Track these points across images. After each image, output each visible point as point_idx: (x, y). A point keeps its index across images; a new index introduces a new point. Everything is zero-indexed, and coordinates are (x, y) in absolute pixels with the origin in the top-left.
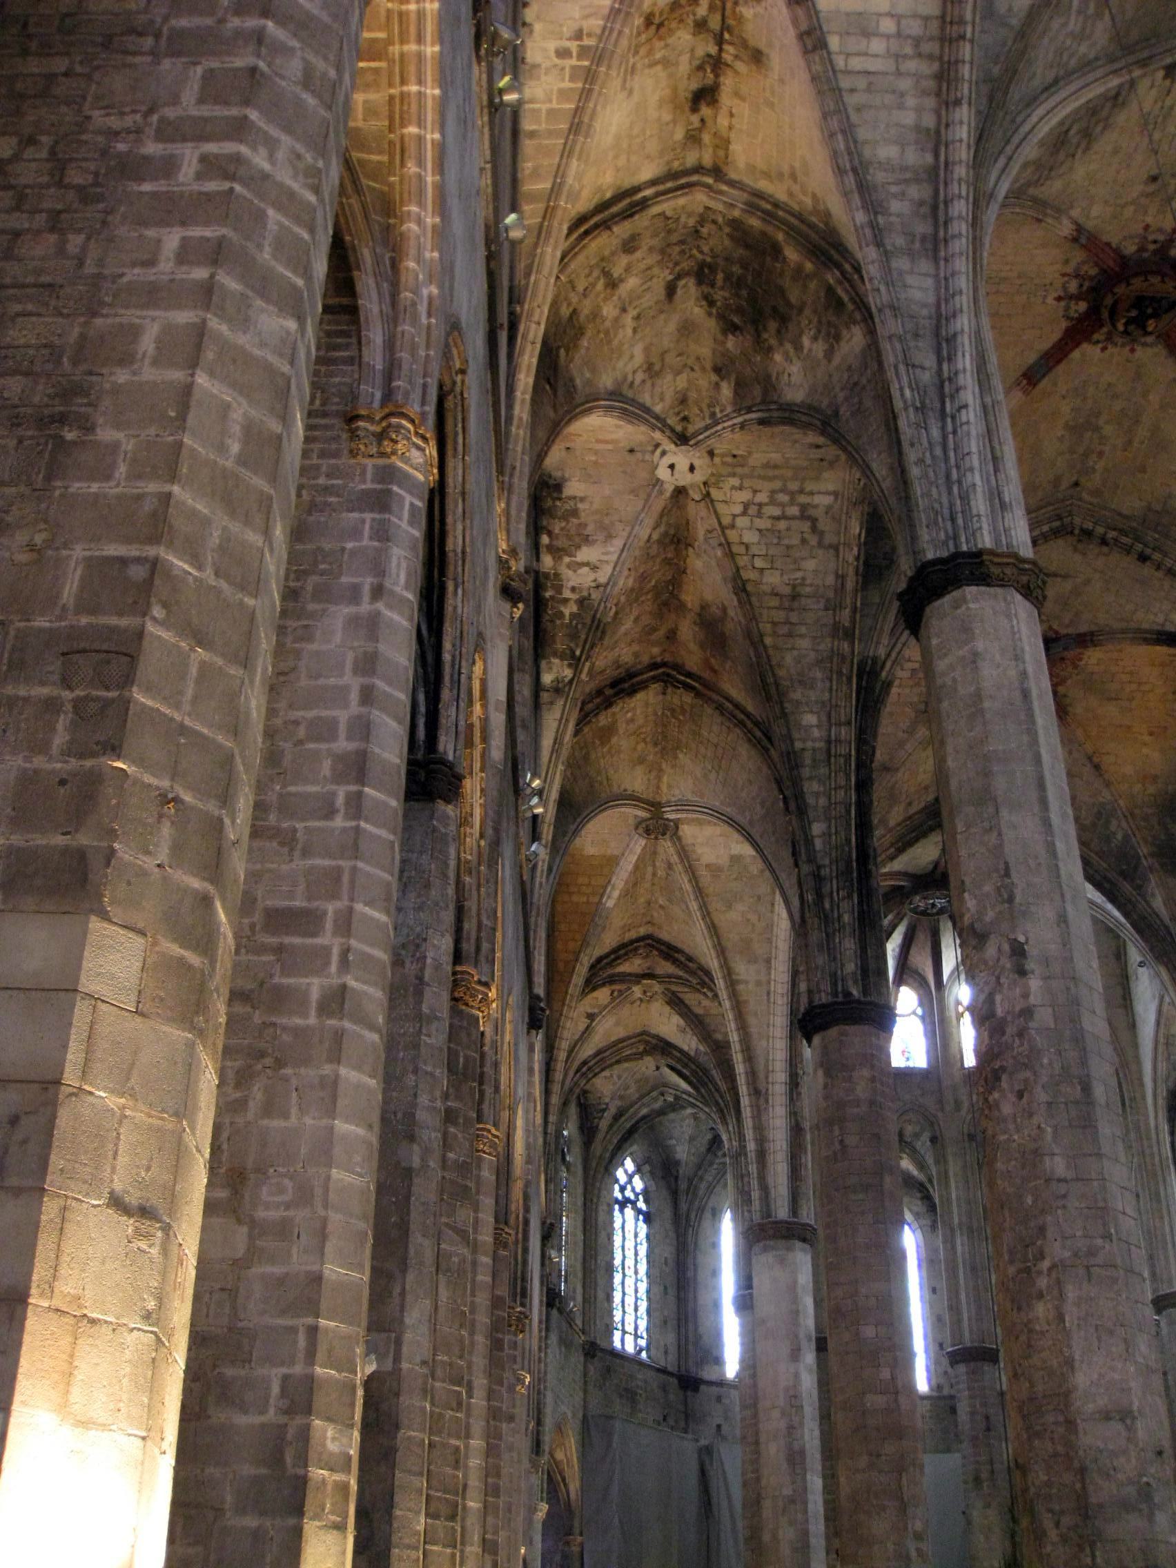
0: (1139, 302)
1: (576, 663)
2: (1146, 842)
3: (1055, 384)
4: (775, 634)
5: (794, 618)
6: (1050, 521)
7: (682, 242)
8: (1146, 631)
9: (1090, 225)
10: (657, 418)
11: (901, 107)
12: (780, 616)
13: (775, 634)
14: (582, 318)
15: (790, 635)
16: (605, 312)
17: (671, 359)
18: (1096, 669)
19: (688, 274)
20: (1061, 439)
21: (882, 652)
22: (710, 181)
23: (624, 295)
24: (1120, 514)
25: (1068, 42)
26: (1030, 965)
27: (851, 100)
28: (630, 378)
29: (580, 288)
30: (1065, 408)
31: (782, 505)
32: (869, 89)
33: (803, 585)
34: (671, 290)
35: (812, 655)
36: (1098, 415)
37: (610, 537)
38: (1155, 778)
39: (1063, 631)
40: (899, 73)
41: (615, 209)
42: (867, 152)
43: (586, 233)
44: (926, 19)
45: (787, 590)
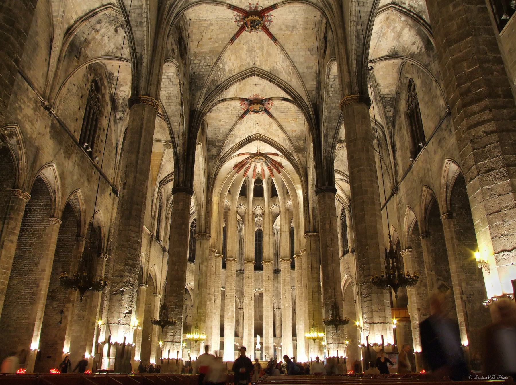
0: (252, 22)
1: (123, 113)
2: (293, 146)
5: (170, 101)
6: (249, 73)
7: (113, 20)
8: (280, 97)
9: (234, 4)
10: (124, 59)
12: (167, 101)
14: (89, 40)
15: (169, 105)
16: (97, 37)
18: (277, 106)
19: (119, 27)
20: (246, 54)
21: (199, 106)
22: (112, 6)
23: (102, 33)
24: (265, 71)
26: (126, 187)
28: (111, 51)
29: (87, 33)
30: (245, 47)
34: (116, 31)
35: (175, 110)
36: (254, 47)
37: (126, 85)
39: (265, 97)
41: (89, 15)
43: (82, 21)
45: (167, 95)
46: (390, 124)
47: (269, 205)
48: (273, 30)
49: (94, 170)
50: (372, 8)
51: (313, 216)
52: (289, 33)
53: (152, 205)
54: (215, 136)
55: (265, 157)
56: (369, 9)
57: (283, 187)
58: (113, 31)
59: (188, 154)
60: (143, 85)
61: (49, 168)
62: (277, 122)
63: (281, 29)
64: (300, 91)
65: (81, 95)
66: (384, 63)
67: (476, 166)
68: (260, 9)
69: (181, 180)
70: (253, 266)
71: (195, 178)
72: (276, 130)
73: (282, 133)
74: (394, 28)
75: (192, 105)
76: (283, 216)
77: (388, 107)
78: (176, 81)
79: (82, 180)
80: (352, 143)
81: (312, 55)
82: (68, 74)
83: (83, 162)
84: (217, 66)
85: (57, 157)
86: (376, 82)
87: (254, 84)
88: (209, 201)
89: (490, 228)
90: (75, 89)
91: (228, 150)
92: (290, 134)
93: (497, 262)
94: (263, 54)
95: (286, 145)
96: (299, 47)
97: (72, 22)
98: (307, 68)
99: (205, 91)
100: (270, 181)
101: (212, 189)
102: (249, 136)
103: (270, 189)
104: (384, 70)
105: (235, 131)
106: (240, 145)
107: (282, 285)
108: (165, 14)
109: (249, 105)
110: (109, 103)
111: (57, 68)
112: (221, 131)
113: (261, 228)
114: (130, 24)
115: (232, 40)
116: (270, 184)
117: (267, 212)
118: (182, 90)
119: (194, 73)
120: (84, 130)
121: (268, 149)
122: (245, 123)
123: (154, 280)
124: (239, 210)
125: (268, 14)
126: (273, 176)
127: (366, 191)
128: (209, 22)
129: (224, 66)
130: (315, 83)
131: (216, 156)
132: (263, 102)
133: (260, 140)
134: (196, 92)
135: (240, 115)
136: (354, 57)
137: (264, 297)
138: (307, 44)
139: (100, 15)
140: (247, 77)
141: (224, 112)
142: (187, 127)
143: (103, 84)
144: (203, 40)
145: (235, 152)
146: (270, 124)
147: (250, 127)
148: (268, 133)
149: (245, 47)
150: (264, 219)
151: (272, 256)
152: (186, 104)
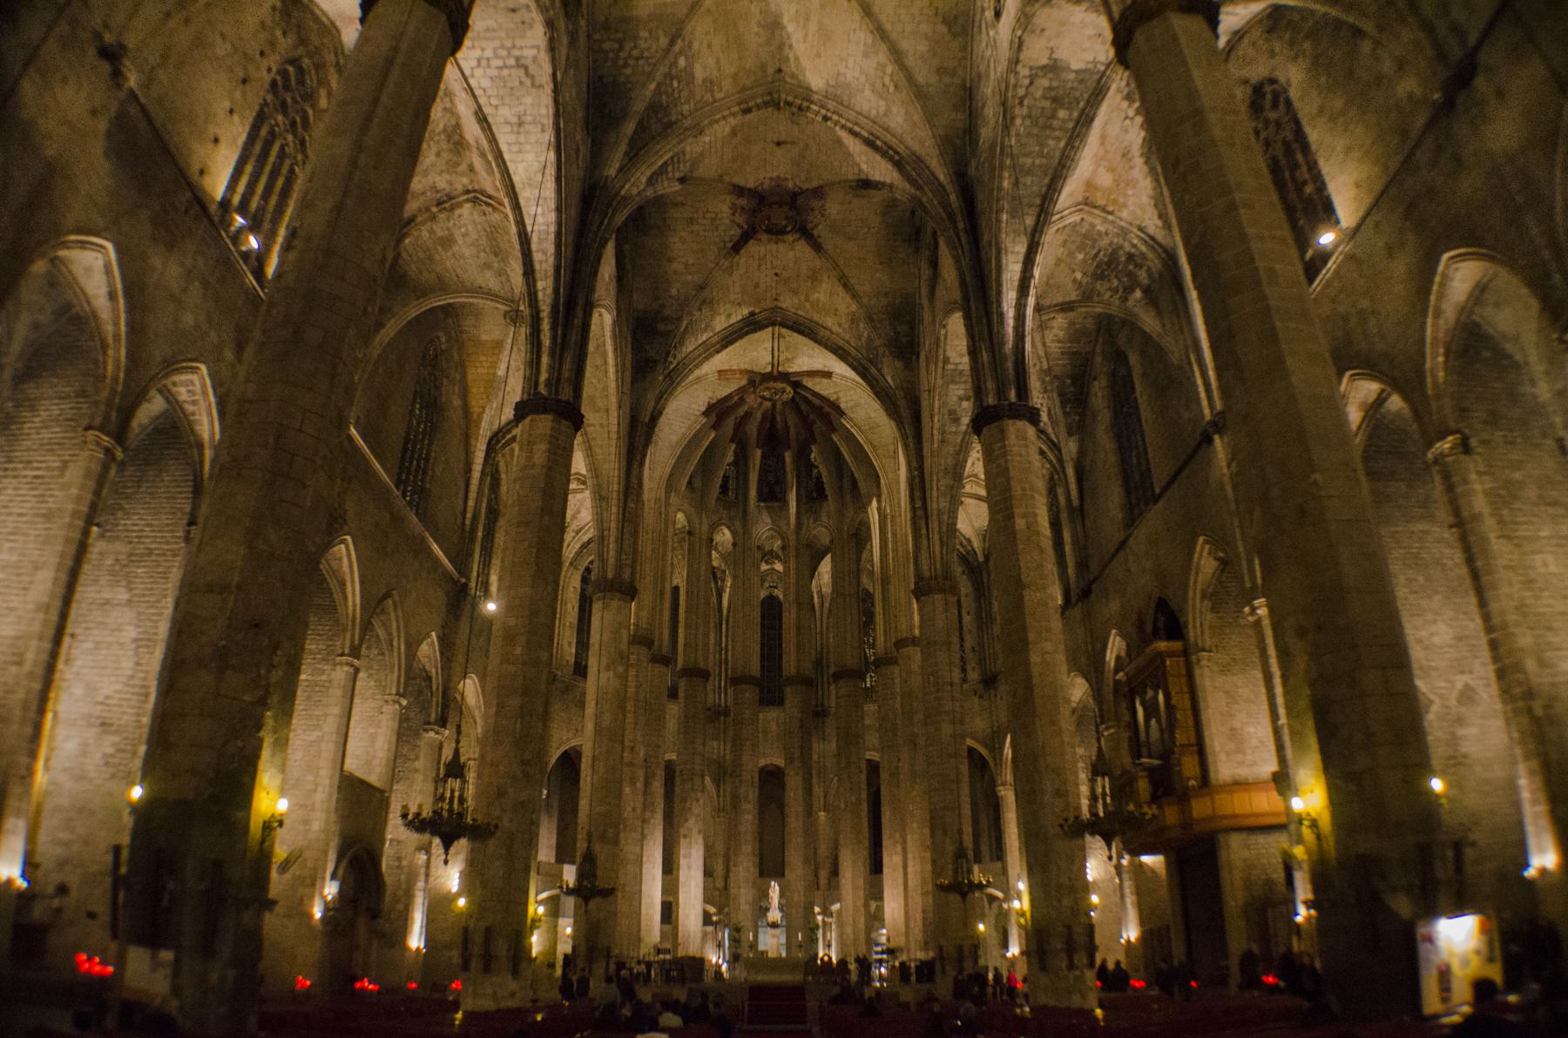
4: (510, 151)
5: (522, 139)
13: (510, 151)
15: (520, 151)
20: (757, 34)
31: (502, 58)
33: (525, 115)
38: (886, 294)
39: (805, 187)
53: (466, 498)
59: (570, 304)
62: (836, 266)
65: (241, 74)
69: (544, 376)
73: (848, 299)
81: (955, 36)
84: (671, 57)
87: (776, 140)
91: (690, 349)
94: (806, 36)
99: (629, 127)
102: (752, 314)
106: (723, 339)
112: (674, 292)
113: (779, 593)
119: (601, 78)
129: (691, 59)
131: (655, 362)
132: (800, 201)
133: (783, 325)
135: (729, 245)
140: (758, 107)
141: (683, 234)
148: (807, 305)
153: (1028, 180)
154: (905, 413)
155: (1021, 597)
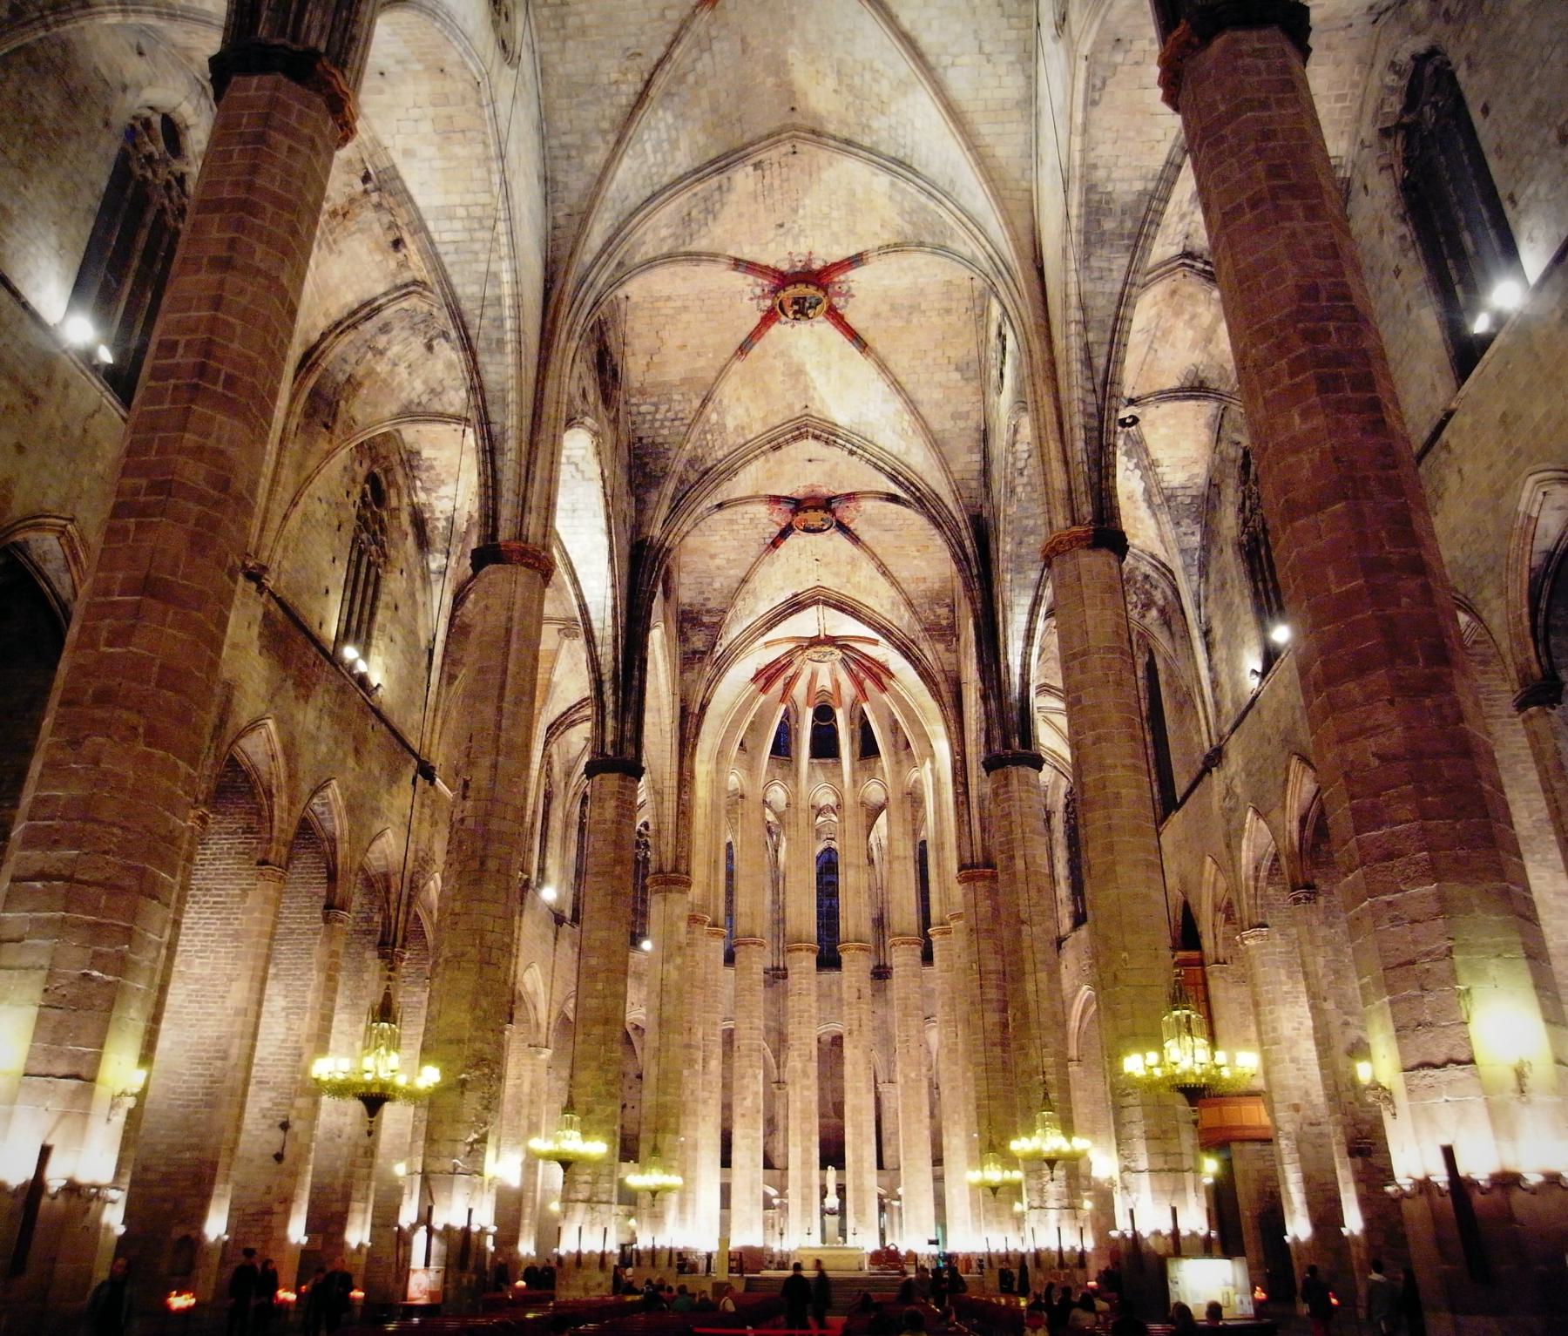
0: (796, 301)
2: (920, 620)
3: (765, 351)
9: (747, 257)
11: (477, 261)
16: (379, 369)
17: (448, 382)
20: (783, 382)
21: (656, 531)
25: (654, 170)
26: (469, 793)
27: (446, 260)
30: (779, 364)
32: (456, 251)
34: (430, 348)
40: (472, 240)
42: (459, 291)
44: (484, 206)
46: (1195, 570)
47: (855, 782)
48: (853, 319)
49: (373, 720)
50: (1125, 284)
51: (981, 819)
52: (900, 324)
54: (700, 599)
55: (842, 647)
56: (1118, 287)
57: (895, 728)
58: (423, 350)
60: (506, 512)
61: (255, 734)
62: (873, 556)
63: (877, 315)
64: (935, 480)
65: (336, 523)
66: (1167, 407)
67: (1360, 846)
68: (817, 265)
69: (609, 738)
70: (813, 957)
71: (649, 718)
72: (872, 578)
74: (1193, 317)
75: (637, 527)
76: (896, 815)
77: (1185, 522)
78: (593, 469)
79: (340, 754)
80: (1076, 663)
82: (304, 475)
83: (342, 705)
85: (278, 700)
86: (1148, 455)
88: (685, 779)
89: (1392, 1003)
90: (320, 510)
92: (910, 588)
93: (1410, 1092)
95: (901, 619)
96: (929, 361)
97: (315, 336)
98: (956, 416)
99: (670, 487)
100: (857, 713)
101: (695, 746)
103: (858, 734)
104: (1172, 422)
105: (756, 582)
107: (897, 1014)
108: (564, 309)
109: (794, 512)
110: (410, 530)
111: (278, 464)
112: (717, 585)
113: (834, 845)
114: (470, 347)
115: (743, 349)
116: (857, 721)
117: (849, 800)
118: (609, 492)
119: (640, 439)
120: (344, 617)
121: (847, 626)
122: (783, 560)
123: (530, 1007)
124: (771, 797)
125: (842, 278)
126: (866, 699)
127: (1117, 796)
128: (679, 304)
130: (977, 457)
131: (704, 653)
133: (826, 603)
134: (648, 491)
136: (1078, 419)
137: (848, 1051)
138: (951, 353)
139: (387, 313)
140: (787, 442)
142: (625, 591)
143: (392, 484)
144: (663, 351)
145: (756, 639)
146: (853, 562)
147: (798, 571)
149: (779, 364)
150: (842, 821)
151: (867, 929)
152: (621, 528)
153: (1032, 539)
154: (947, 697)
155: (1019, 932)
